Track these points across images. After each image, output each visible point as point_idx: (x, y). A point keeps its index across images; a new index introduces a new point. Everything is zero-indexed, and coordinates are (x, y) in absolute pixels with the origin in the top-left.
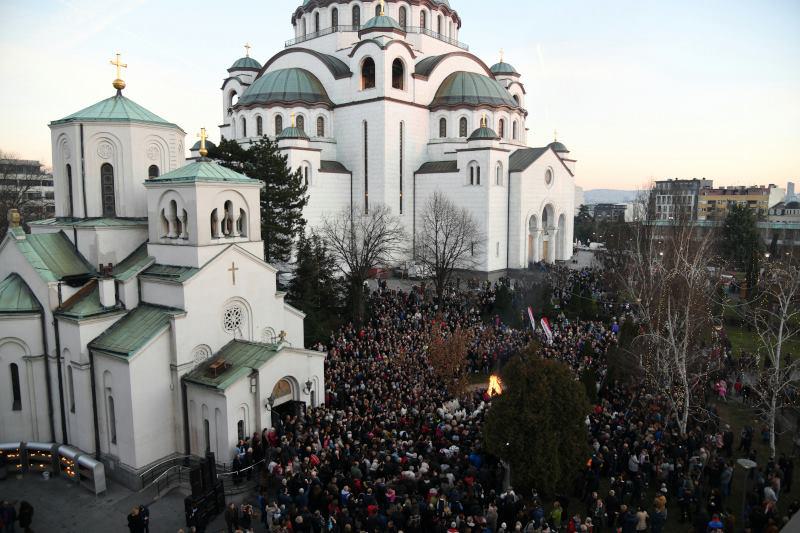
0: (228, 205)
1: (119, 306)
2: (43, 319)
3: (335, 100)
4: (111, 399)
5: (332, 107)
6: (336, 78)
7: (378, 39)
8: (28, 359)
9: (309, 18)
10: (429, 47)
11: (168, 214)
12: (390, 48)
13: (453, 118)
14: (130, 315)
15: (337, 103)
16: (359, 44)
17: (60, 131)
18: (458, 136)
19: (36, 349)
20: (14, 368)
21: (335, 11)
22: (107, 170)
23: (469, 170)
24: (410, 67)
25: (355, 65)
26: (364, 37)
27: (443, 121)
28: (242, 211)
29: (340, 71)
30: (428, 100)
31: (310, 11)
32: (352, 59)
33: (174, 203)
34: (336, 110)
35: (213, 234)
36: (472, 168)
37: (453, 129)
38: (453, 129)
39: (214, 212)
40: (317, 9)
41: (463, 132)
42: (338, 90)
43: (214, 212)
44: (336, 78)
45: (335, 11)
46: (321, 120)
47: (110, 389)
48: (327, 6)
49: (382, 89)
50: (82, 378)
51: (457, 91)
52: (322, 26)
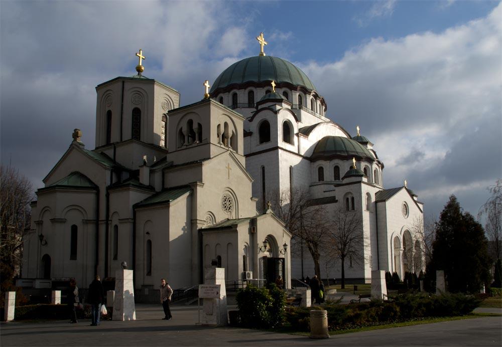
0: (226, 124)
4: (150, 242)
7: (271, 107)
8: (86, 222)
10: (307, 119)
11: (185, 130)
13: (328, 167)
18: (333, 180)
19: (91, 216)
20: (74, 229)
22: (137, 113)
23: (345, 200)
24: (296, 127)
26: (260, 107)
27: (321, 170)
32: (253, 122)
33: (190, 123)
36: (348, 199)
37: (329, 175)
38: (329, 175)
39: (219, 126)
41: (337, 176)
47: (148, 233)
48: (229, 92)
49: (277, 142)
50: (125, 231)
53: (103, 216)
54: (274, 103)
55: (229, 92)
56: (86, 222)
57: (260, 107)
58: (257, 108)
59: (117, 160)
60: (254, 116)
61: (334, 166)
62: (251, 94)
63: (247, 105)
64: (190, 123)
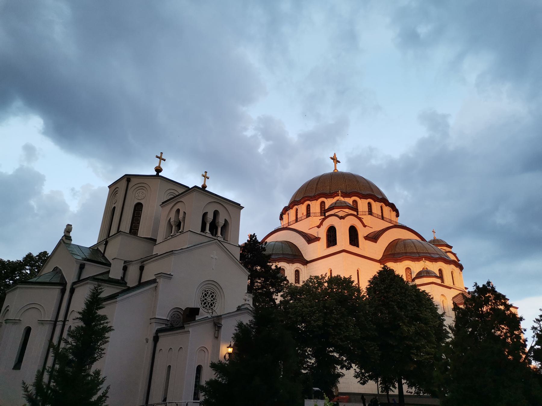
0: (216, 213)
1: (121, 282)
2: (63, 292)
3: (308, 258)
5: (305, 263)
8: (42, 322)
9: (292, 212)
14: (129, 290)
15: (308, 260)
16: (324, 220)
17: (114, 187)
19: (49, 316)
20: (28, 330)
21: (308, 207)
24: (362, 232)
25: (322, 233)
26: (327, 214)
28: (226, 221)
29: (310, 239)
30: (379, 257)
33: (178, 210)
34: (308, 265)
35: (203, 229)
39: (205, 215)
43: (205, 215)
45: (308, 207)
46: (297, 273)
48: (303, 203)
51: (400, 249)
53: (61, 318)
56: (42, 322)
57: (327, 214)
58: (325, 215)
59: (106, 255)
60: (321, 224)
61: (405, 268)
62: (323, 203)
63: (319, 214)
64: (178, 210)
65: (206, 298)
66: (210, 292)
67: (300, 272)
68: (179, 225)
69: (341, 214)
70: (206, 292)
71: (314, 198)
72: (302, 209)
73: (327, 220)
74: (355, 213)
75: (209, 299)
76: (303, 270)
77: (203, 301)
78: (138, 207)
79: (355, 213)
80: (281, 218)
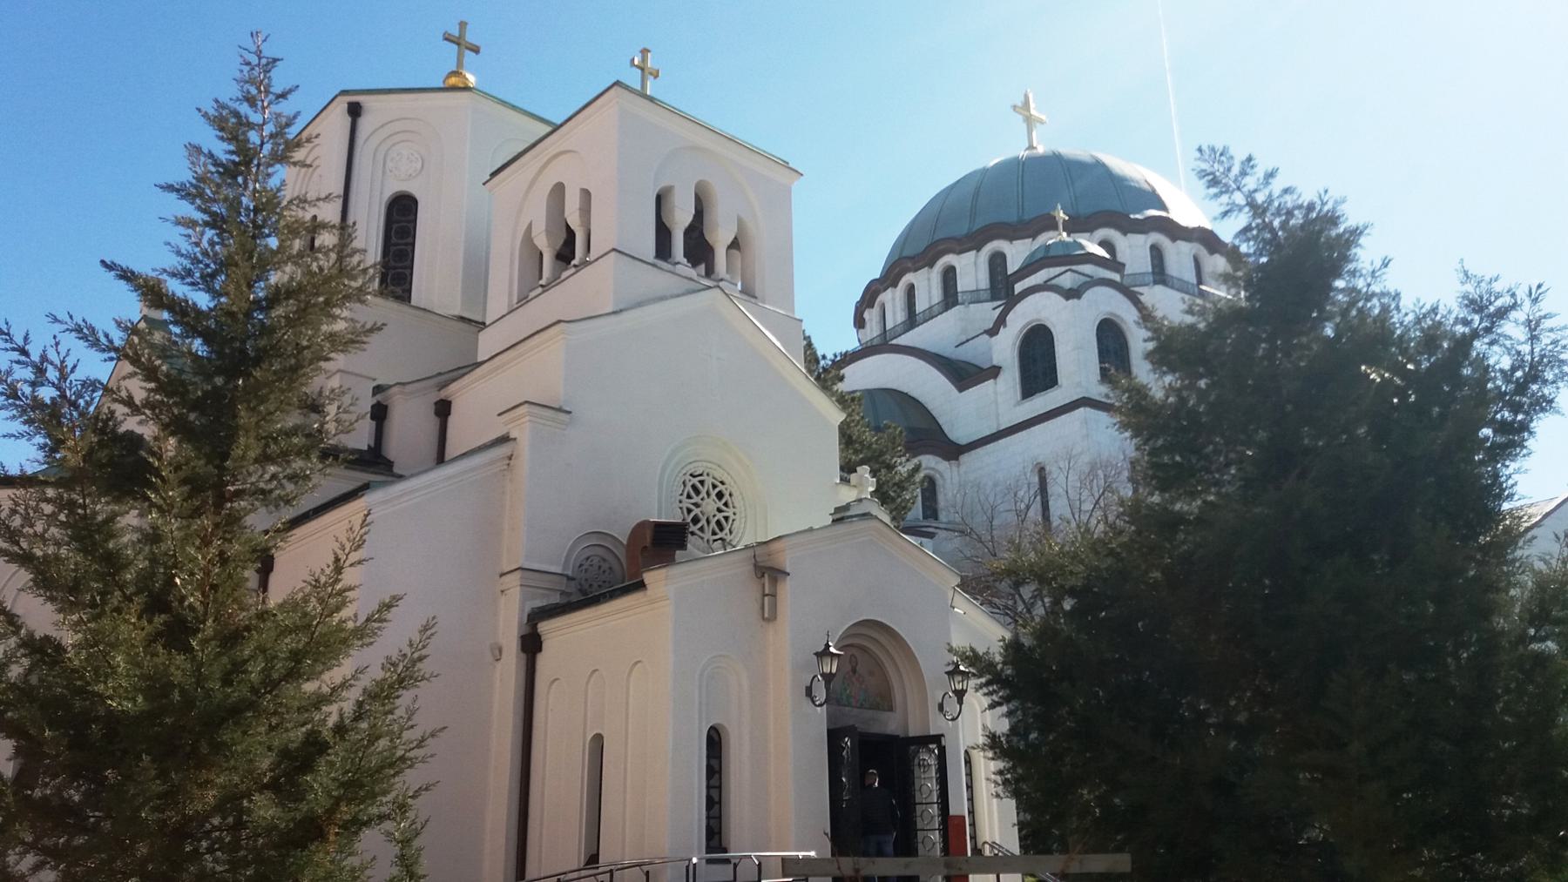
3: (960, 432)
5: (954, 451)
6: (961, 390)
9: (893, 300)
12: (1090, 295)
15: (963, 442)
21: (949, 275)
25: (1005, 349)
26: (1018, 288)
31: (895, 285)
33: (559, 190)
34: (964, 458)
40: (909, 278)
42: (961, 412)
44: (961, 390)
52: (921, 306)
54: (1063, 269)
55: (931, 265)
57: (1018, 288)
60: (1001, 322)
62: (998, 260)
63: (987, 295)
64: (559, 190)
65: (696, 499)
66: (709, 481)
67: (939, 482)
68: (565, 255)
69: (1067, 281)
70: (695, 481)
71: (973, 241)
72: (927, 285)
73: (1019, 308)
74: (1116, 277)
75: (710, 506)
76: (947, 475)
77: (689, 511)
78: (402, 211)
79: (1116, 277)
80: (859, 323)
